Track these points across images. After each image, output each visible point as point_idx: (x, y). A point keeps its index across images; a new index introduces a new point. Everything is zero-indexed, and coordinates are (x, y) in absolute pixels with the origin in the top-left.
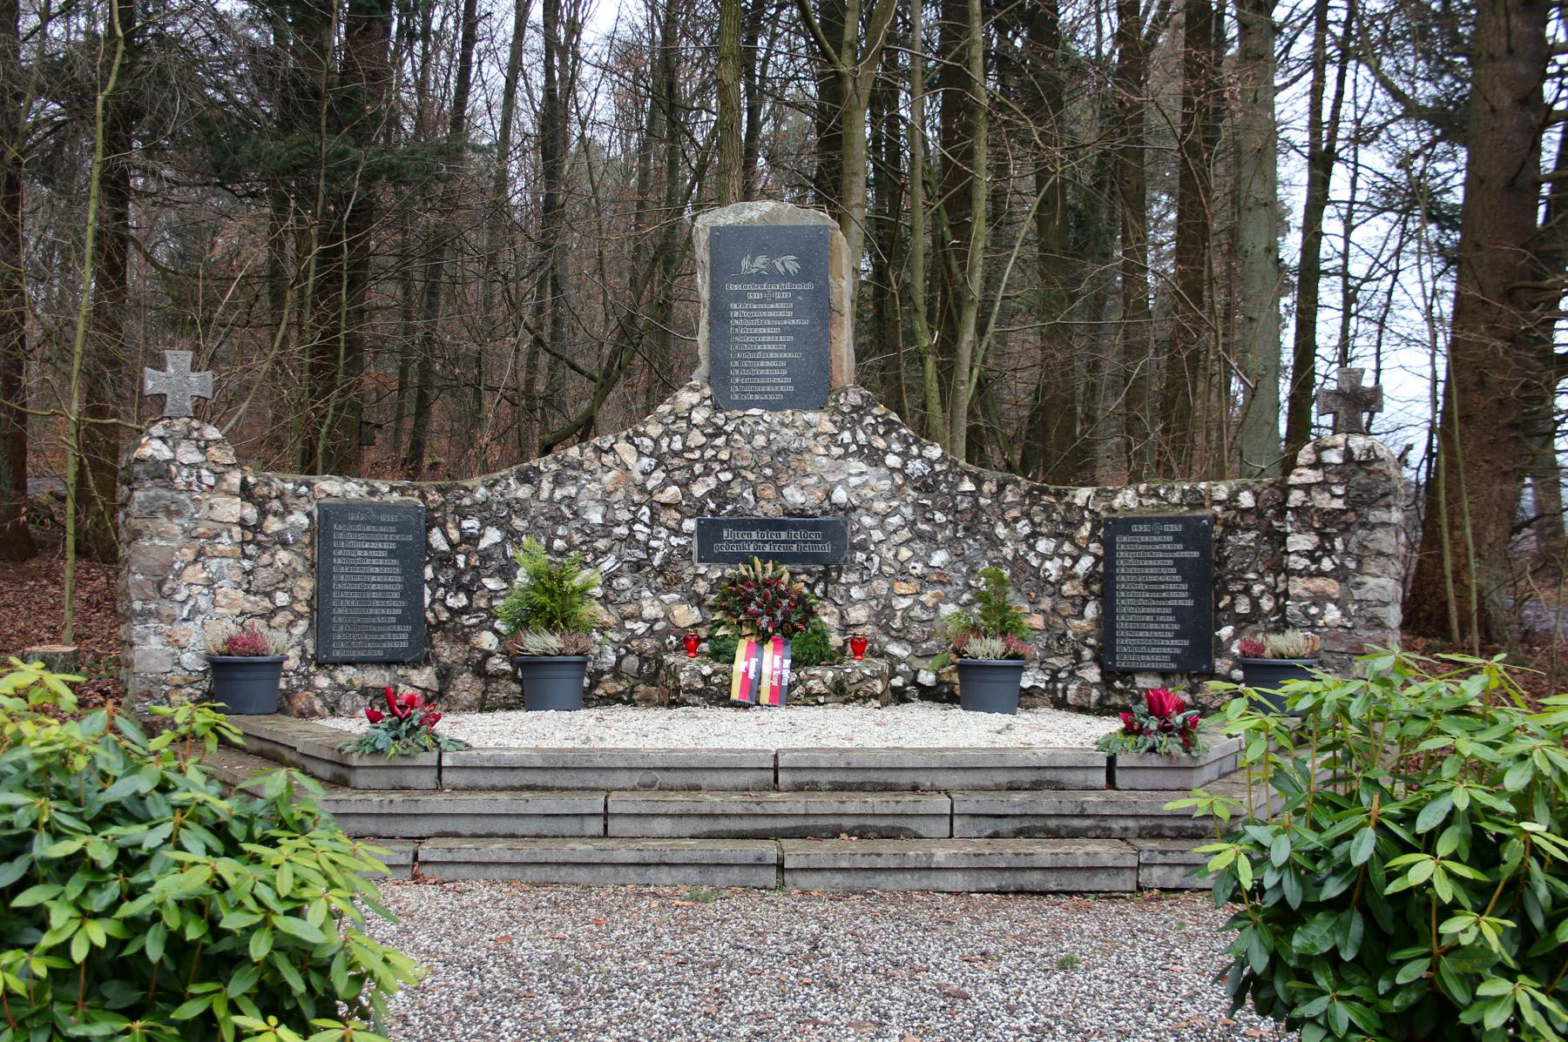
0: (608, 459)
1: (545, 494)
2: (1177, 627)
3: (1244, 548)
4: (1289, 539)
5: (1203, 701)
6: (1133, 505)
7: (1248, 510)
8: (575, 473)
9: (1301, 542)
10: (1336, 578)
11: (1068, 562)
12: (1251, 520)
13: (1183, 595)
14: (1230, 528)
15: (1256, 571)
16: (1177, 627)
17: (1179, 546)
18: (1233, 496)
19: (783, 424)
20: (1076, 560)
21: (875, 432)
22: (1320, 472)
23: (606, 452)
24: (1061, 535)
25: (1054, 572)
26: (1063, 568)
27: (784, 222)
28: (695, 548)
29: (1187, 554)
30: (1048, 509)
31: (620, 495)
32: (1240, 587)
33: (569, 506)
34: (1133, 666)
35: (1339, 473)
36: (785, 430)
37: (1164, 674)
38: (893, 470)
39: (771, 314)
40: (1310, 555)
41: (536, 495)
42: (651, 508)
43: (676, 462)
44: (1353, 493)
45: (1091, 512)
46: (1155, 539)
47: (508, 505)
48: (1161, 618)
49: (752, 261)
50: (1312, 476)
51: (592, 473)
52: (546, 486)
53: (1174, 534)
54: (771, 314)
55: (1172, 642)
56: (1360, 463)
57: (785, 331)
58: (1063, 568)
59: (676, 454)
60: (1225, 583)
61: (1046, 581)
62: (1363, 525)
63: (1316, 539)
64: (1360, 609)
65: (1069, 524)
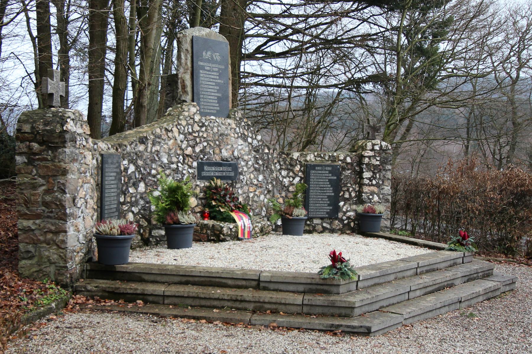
0: (170, 134)
1: (149, 150)
2: (328, 202)
3: (347, 176)
4: (364, 174)
5: (333, 227)
6: (313, 160)
7: (349, 163)
8: (159, 140)
9: (367, 175)
10: (377, 187)
11: (291, 179)
12: (349, 167)
13: (331, 191)
14: (344, 169)
15: (350, 184)
16: (328, 202)
17: (330, 175)
18: (345, 158)
19: (222, 123)
20: (294, 178)
21: (245, 128)
22: (373, 153)
23: (169, 131)
24: (289, 169)
25: (287, 183)
26: (290, 182)
27: (213, 38)
28: (196, 174)
29: (332, 178)
30: (284, 160)
31: (173, 151)
32: (346, 189)
33: (157, 155)
34: (314, 216)
35: (378, 153)
36: (223, 126)
37: (322, 218)
38: (249, 143)
39: (212, 77)
40: (370, 179)
41: (146, 149)
42: (183, 157)
43: (190, 137)
44: (382, 160)
45: (300, 161)
46: (323, 172)
47: (136, 154)
48: (324, 199)
49: (206, 53)
50: (371, 153)
51: (164, 140)
52: (150, 145)
53: (329, 171)
54: (212, 77)
55: (327, 208)
56: (384, 150)
57: (217, 84)
58: (290, 182)
59: (190, 134)
60: (341, 187)
61: (284, 186)
62: (384, 170)
63: (372, 174)
64: (383, 197)
65: (291, 165)
